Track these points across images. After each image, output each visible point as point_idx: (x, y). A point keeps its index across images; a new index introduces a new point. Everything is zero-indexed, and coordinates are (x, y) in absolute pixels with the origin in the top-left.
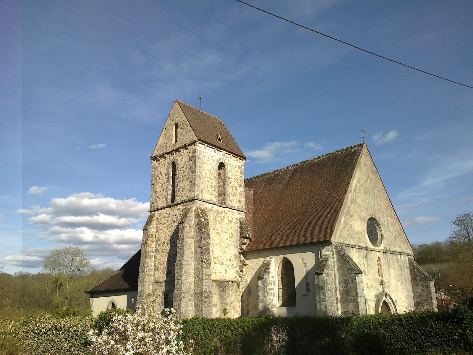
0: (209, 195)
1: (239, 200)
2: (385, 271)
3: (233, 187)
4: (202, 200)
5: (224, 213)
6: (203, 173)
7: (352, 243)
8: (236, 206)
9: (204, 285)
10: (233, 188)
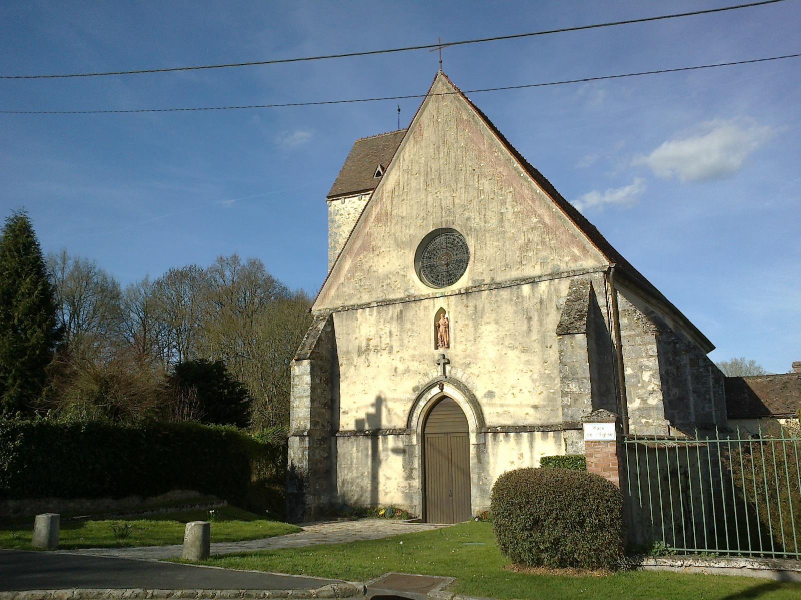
2: (459, 334)
7: (366, 299)
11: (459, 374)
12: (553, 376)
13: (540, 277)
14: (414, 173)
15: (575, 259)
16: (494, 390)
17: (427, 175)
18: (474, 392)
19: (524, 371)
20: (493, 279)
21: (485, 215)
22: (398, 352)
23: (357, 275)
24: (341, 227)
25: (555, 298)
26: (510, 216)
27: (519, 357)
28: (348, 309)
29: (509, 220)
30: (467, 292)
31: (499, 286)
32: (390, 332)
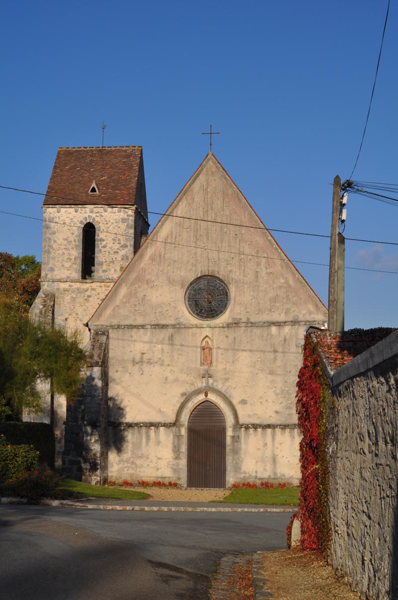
0: (66, 271)
3: (110, 250)
6: (55, 246)
7: (139, 321)
10: (109, 253)
11: (219, 386)
12: (290, 392)
13: (285, 322)
14: (185, 226)
15: (310, 313)
16: (246, 399)
17: (197, 231)
18: (231, 399)
19: (270, 387)
20: (248, 319)
21: (244, 270)
22: (169, 365)
23: (132, 300)
24: (55, 233)
25: (295, 339)
26: (263, 273)
27: (267, 378)
28: (125, 328)
29: (263, 278)
30: (228, 326)
31: (253, 325)
32: (162, 349)
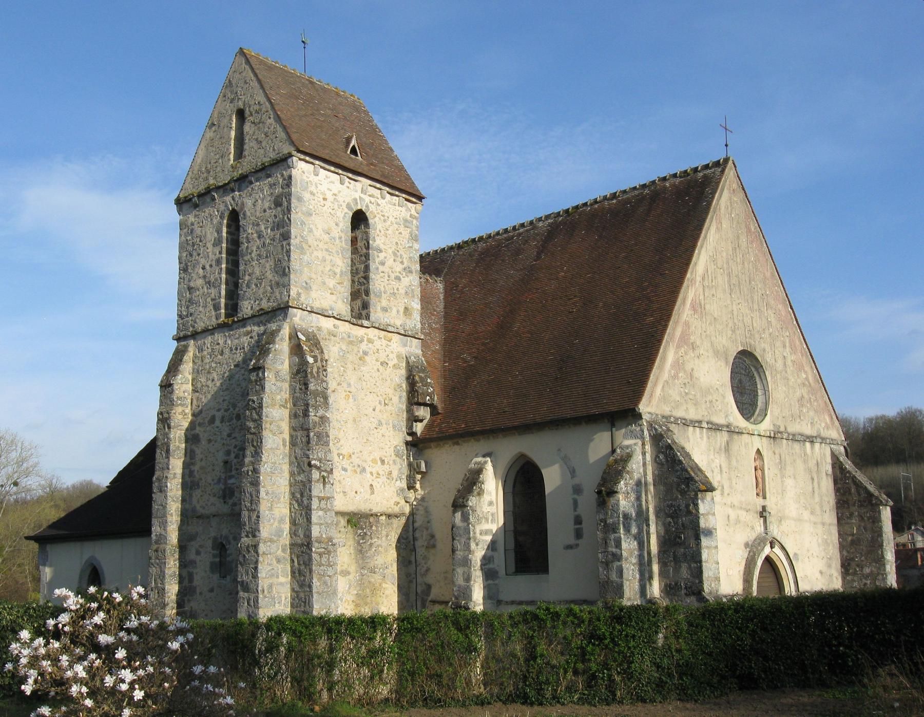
1: (406, 308)
3: (391, 274)
4: (309, 309)
5: (365, 342)
6: (311, 240)
7: (692, 415)
8: (398, 323)
9: (316, 524)
15: (827, 427)
